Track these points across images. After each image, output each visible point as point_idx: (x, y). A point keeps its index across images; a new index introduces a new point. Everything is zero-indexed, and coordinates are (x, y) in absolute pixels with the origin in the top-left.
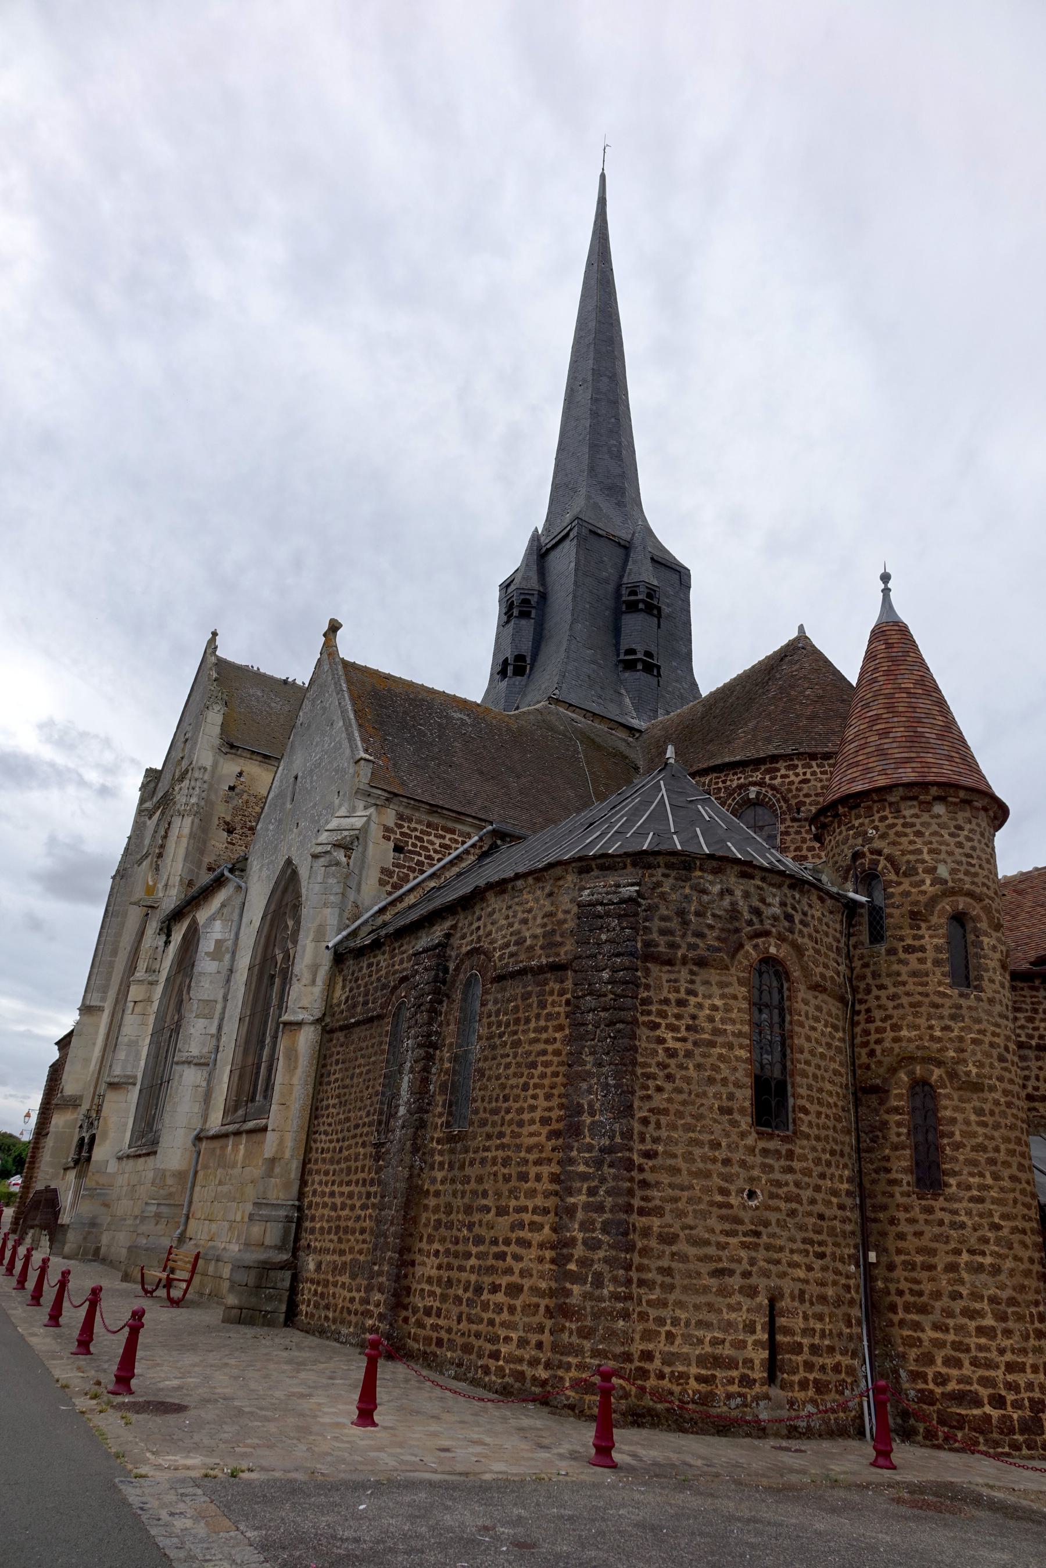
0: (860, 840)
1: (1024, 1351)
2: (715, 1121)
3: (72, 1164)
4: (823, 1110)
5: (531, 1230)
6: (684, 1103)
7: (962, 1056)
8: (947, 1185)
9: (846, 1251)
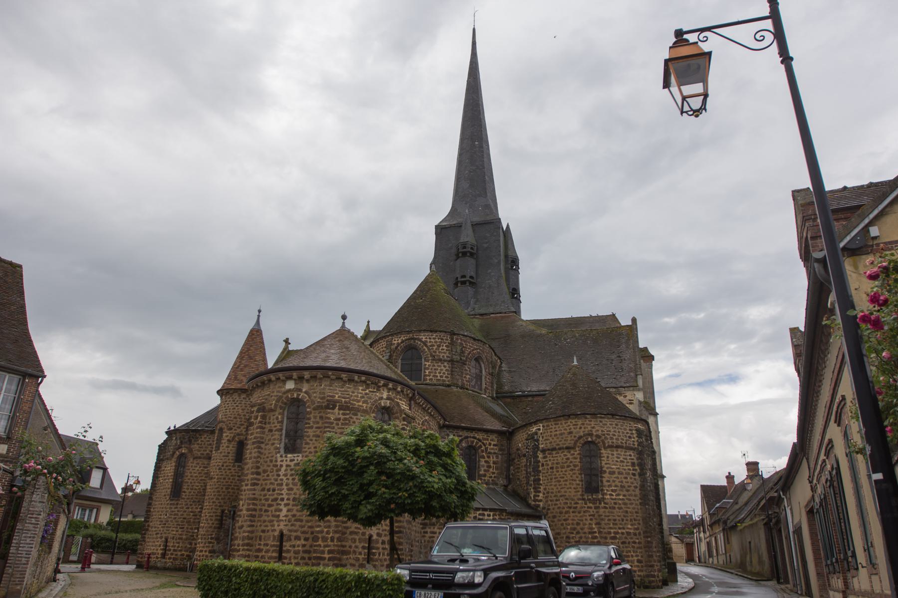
1: (203, 547)
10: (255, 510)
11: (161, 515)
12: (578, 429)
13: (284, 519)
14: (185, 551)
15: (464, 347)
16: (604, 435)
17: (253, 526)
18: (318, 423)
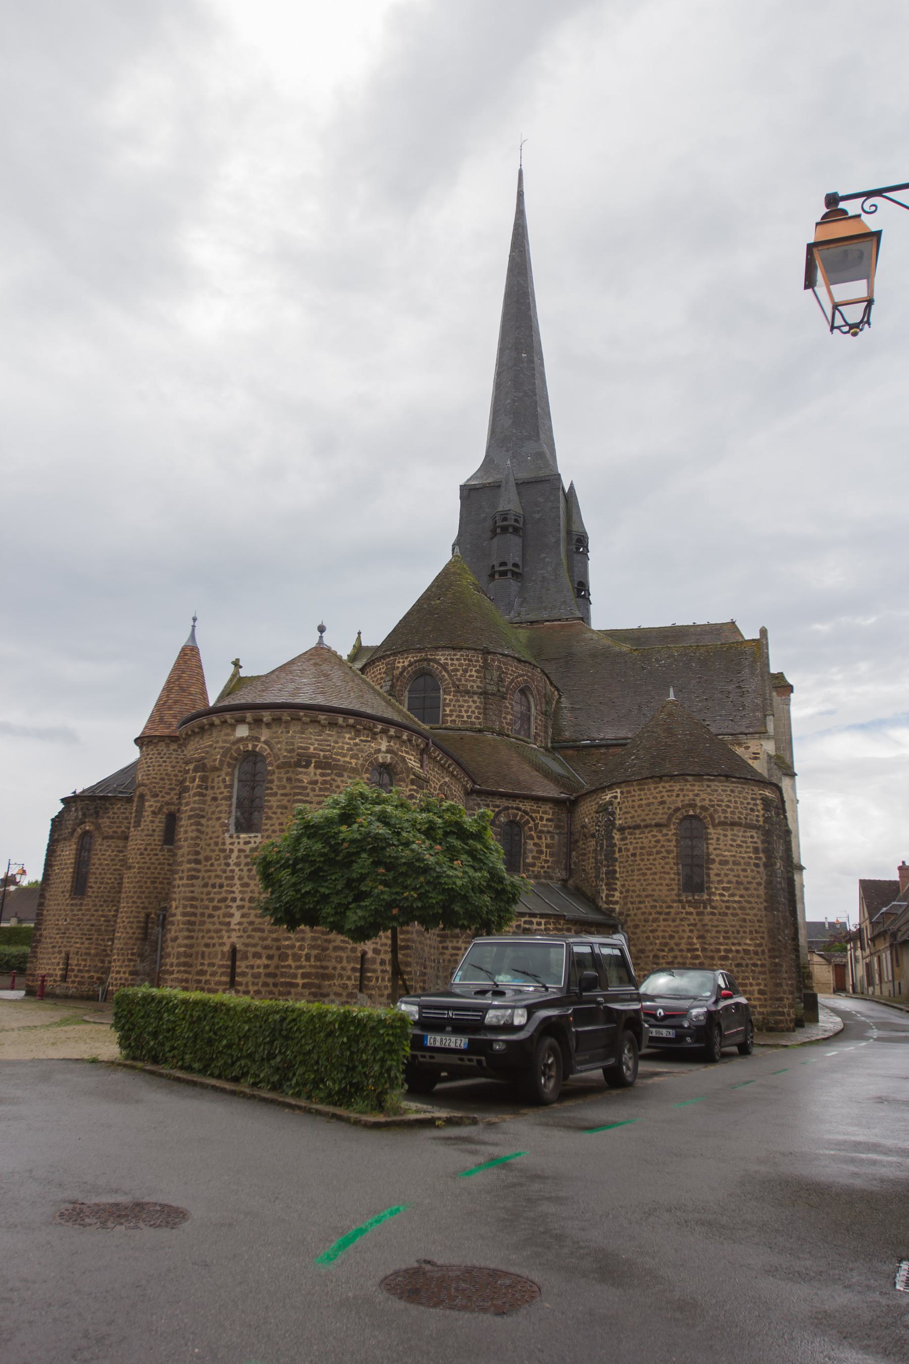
1: (121, 966)
10: (195, 915)
11: (58, 920)
12: (674, 798)
13: (237, 927)
14: (95, 972)
15: (503, 672)
16: (713, 806)
17: (191, 937)
18: (284, 787)
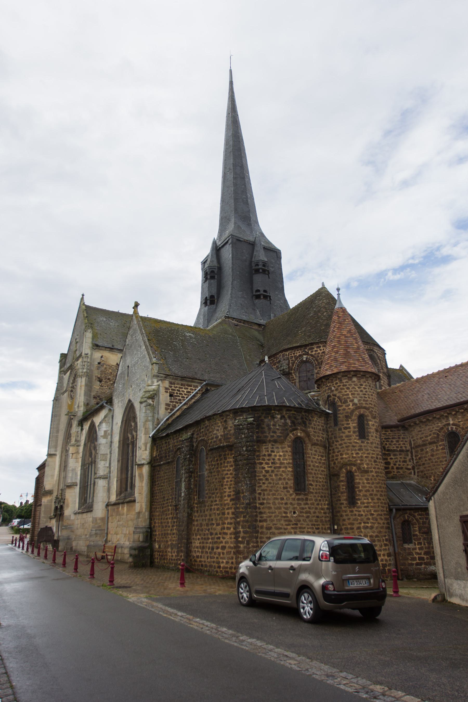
0: (330, 391)
2: (282, 491)
3: (53, 517)
4: (318, 484)
5: (227, 529)
6: (272, 487)
7: (362, 462)
8: (358, 503)
9: (327, 526)
